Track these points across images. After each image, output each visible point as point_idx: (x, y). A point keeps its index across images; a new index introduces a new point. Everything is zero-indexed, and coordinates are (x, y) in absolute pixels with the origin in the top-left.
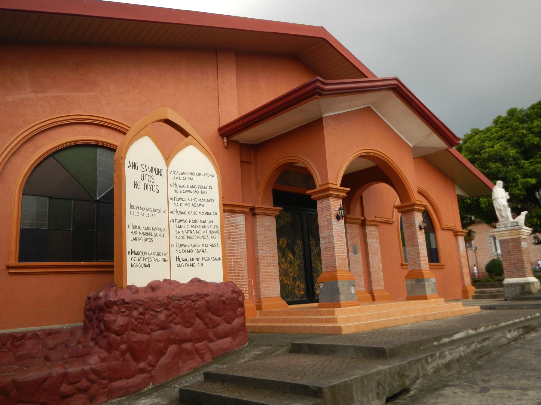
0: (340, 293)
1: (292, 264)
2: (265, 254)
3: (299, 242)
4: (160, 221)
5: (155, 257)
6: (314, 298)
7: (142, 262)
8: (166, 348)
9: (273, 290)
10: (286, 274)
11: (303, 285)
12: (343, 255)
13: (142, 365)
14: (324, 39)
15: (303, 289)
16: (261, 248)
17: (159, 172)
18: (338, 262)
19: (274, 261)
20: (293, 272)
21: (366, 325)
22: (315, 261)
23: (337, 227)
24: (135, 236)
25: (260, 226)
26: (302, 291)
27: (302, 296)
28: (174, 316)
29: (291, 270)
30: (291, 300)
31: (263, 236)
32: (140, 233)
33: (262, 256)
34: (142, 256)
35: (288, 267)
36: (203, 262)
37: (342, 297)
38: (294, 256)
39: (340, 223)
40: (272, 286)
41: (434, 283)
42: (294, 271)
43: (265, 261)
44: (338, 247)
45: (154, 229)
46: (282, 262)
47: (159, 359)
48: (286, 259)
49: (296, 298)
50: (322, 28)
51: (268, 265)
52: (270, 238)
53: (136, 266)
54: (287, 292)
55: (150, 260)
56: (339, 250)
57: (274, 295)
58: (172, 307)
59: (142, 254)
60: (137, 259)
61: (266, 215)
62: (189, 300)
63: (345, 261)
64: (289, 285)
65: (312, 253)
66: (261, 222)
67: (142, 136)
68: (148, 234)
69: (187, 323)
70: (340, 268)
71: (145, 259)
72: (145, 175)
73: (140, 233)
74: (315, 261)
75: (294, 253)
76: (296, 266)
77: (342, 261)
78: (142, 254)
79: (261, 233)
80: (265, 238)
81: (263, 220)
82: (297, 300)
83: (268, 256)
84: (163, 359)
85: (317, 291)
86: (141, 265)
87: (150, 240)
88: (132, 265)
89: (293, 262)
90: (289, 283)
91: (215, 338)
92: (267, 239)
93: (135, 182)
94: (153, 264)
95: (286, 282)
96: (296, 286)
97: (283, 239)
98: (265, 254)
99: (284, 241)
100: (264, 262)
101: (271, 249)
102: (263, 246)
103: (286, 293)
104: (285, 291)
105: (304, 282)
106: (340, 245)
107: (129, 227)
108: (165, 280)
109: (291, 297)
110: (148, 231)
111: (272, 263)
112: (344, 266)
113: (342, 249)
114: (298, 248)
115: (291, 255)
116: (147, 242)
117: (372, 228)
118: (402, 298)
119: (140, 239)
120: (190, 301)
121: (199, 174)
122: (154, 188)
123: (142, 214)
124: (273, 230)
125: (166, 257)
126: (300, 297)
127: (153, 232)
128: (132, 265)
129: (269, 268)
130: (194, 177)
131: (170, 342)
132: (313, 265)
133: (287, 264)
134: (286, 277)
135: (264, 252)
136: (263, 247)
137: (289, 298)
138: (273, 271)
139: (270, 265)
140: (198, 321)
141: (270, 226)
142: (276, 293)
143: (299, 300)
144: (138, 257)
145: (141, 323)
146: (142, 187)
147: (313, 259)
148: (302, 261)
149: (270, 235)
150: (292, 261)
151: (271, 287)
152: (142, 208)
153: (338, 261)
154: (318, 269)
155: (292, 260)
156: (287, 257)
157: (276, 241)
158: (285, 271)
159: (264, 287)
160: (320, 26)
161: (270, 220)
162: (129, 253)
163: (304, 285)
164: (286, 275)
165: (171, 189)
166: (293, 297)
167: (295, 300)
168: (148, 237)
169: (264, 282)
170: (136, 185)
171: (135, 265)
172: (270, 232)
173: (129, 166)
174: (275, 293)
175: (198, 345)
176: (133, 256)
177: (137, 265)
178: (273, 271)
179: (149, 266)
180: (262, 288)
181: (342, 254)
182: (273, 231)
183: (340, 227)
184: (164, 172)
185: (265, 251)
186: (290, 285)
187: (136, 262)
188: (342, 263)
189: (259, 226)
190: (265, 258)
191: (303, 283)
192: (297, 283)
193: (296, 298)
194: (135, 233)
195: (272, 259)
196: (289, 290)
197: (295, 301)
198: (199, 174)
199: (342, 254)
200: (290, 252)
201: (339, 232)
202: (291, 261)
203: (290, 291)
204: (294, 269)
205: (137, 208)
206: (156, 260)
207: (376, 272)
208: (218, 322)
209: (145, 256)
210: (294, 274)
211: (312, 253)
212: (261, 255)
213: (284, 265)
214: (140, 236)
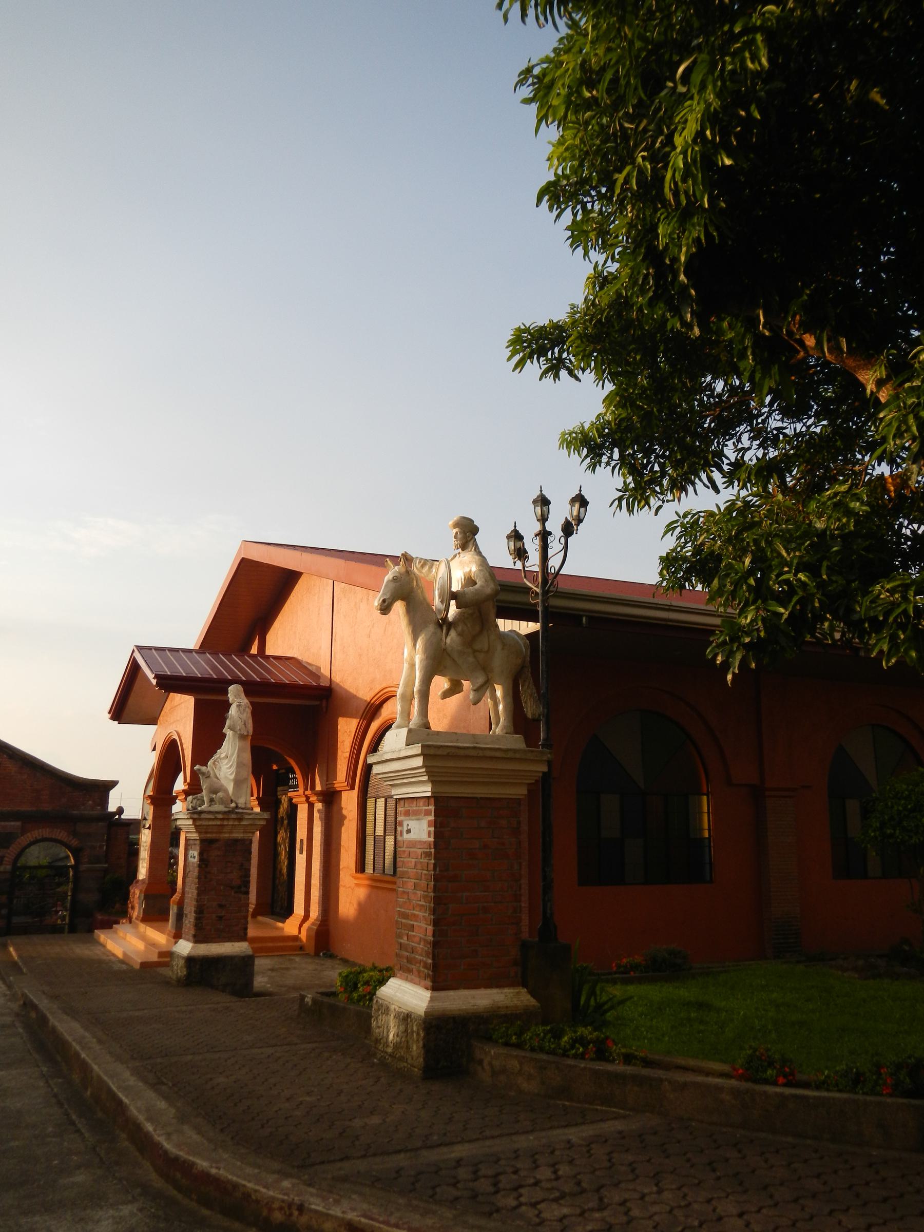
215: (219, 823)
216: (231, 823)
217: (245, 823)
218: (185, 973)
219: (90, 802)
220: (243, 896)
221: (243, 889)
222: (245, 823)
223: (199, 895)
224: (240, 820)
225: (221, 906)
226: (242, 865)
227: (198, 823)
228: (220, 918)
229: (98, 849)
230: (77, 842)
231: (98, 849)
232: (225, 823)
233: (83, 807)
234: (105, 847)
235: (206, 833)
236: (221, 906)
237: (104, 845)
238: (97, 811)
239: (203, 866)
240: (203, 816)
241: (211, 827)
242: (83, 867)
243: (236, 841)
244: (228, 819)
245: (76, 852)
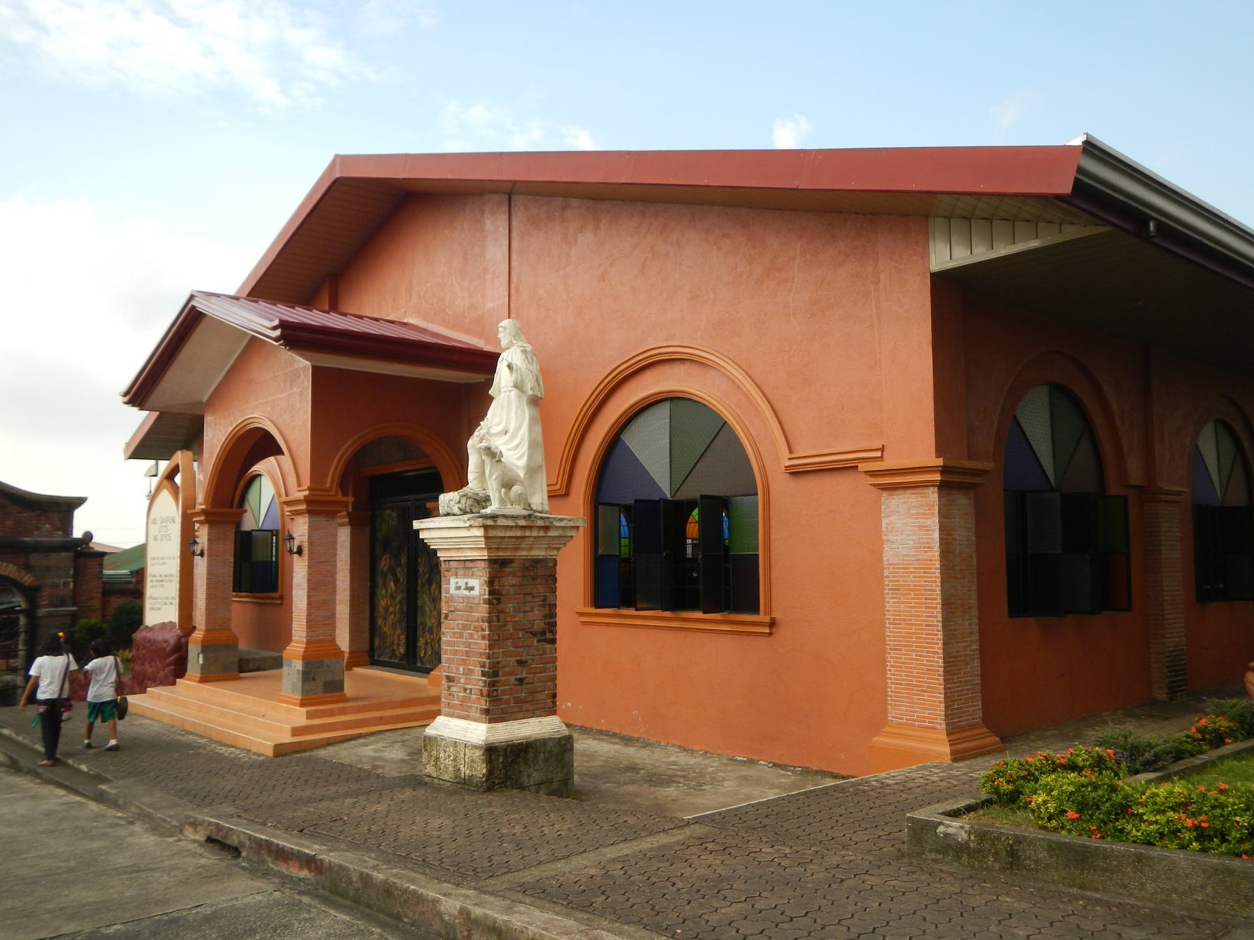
6: (415, 663)
38: (396, 585)
41: (298, 671)
45: (166, 576)
48: (386, 591)
50: (337, 157)
67: (161, 491)
82: (396, 661)
87: (162, 586)
94: (164, 607)
105: (405, 633)
114: (401, 573)
115: (392, 584)
118: (569, 704)
167: (393, 661)
168: (161, 583)
170: (156, 539)
176: (151, 601)
179: (160, 609)
192: (397, 633)
193: (395, 659)
194: (152, 581)
206: (166, 604)
210: (395, 616)
215: (519, 533)
216: (535, 534)
217: (552, 533)
218: (484, 771)
219: (47, 526)
220: (548, 646)
221: (549, 636)
222: (552, 533)
223: (491, 647)
224: (546, 528)
225: (521, 663)
226: (545, 599)
227: (492, 533)
228: (521, 681)
229: (62, 587)
230: (31, 580)
231: (62, 587)
232: (528, 534)
233: (36, 533)
234: (71, 585)
235: (498, 549)
236: (521, 663)
237: (69, 582)
238: (58, 537)
239: (495, 602)
240: (501, 522)
241: (507, 540)
242: (42, 612)
243: (536, 562)
244: (530, 528)
245: (31, 594)
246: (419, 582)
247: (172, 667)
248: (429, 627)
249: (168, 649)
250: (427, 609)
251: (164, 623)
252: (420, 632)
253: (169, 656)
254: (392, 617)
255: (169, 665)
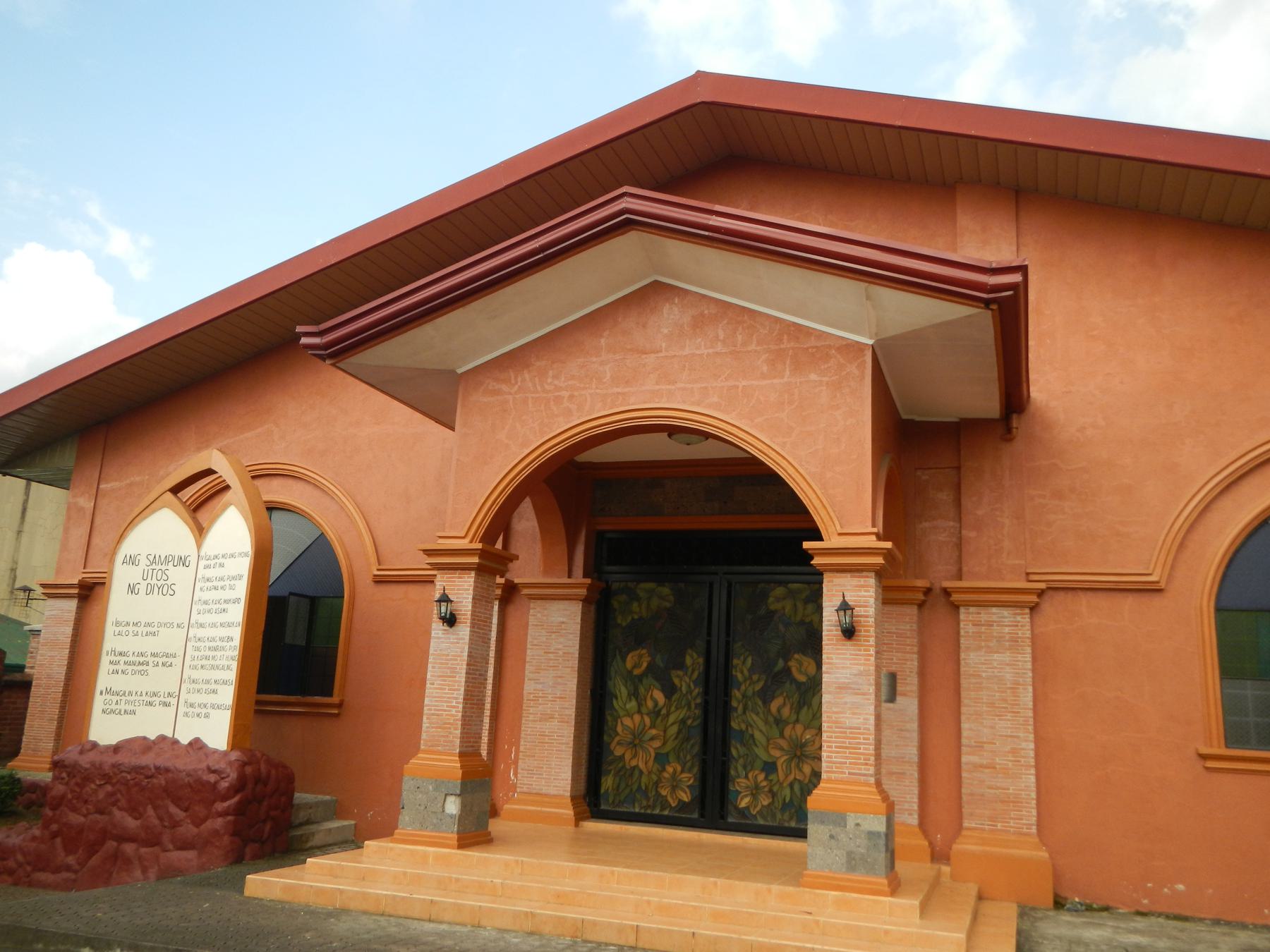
0: (403, 808)
1: (660, 719)
2: (542, 690)
3: (694, 660)
4: (170, 641)
5: (149, 699)
6: (723, 817)
7: (123, 707)
8: (102, 843)
9: (550, 779)
10: (637, 742)
11: (691, 775)
12: (447, 715)
13: (71, 860)
14: (703, 102)
15: (688, 787)
16: (532, 676)
17: (183, 561)
18: (426, 732)
19: (563, 708)
20: (662, 738)
21: (320, 892)
22: (744, 712)
23: (443, 642)
24: (115, 667)
25: (537, 625)
26: (686, 793)
27: (683, 806)
28: (119, 796)
29: (654, 732)
30: (643, 811)
31: (542, 649)
32: (125, 663)
33: (532, 695)
34: (123, 698)
35: (645, 726)
36: (210, 710)
37: (407, 818)
39: (453, 634)
40: (550, 768)
41: (871, 835)
42: (664, 737)
43: (538, 707)
44: (437, 693)
45: (153, 655)
46: (627, 710)
47: (90, 858)
48: (640, 705)
49: (663, 809)
51: (547, 717)
52: (561, 653)
53: (110, 713)
54: (635, 787)
55: (137, 704)
56: (436, 701)
57: (552, 791)
58: (118, 782)
59: (124, 694)
60: (114, 703)
61: (555, 599)
62: (141, 774)
63: (450, 728)
64: (641, 772)
65: (739, 690)
66: (539, 615)
68: (142, 664)
69: (134, 811)
70: (432, 746)
71: (129, 702)
72: (150, 572)
73: (125, 663)
74: (744, 712)
75: (669, 690)
76: (672, 724)
77: (440, 728)
78: (124, 694)
79: (535, 642)
80: (545, 653)
81: (546, 612)
82: (666, 813)
83: (550, 696)
84: (94, 858)
85: (742, 799)
86: (120, 711)
88: (104, 711)
89: (664, 712)
90: (641, 765)
91: (171, 847)
92: (551, 656)
93: (129, 585)
95: (634, 763)
96: (666, 775)
97: (638, 652)
98: (542, 690)
99: (640, 656)
100: (534, 709)
101: (559, 680)
102: (539, 673)
103: (631, 790)
104: (627, 785)
105: (695, 770)
106: (445, 689)
107: (107, 655)
108: (162, 738)
109: (644, 803)
110: (142, 659)
111: (557, 714)
112: (445, 741)
113: (448, 698)
115: (659, 696)
116: (138, 676)
117: (994, 614)
119: (123, 672)
120: (142, 777)
121: (232, 556)
122: (167, 589)
123: (135, 632)
124: (571, 634)
125: (168, 700)
126: (676, 807)
127: (150, 659)
128: (104, 711)
129: (548, 724)
130: (227, 562)
131: (104, 835)
132: (734, 725)
133: (642, 717)
134: (636, 753)
135: (540, 687)
136: (537, 674)
137: (636, 805)
138: (556, 732)
139: (550, 718)
140: (150, 811)
141: (563, 626)
142: (557, 787)
143: (671, 814)
144: (115, 698)
145: (77, 799)
146: (143, 592)
147: (736, 709)
148: (697, 711)
149: (560, 646)
150: (660, 710)
151: (545, 769)
152: (135, 624)
153: (428, 727)
154: (752, 736)
155: (662, 708)
156: (645, 700)
157: (575, 660)
158: (633, 734)
159: (527, 768)
160: (692, 72)
161: (564, 610)
162: (101, 693)
163: (694, 775)
164: (635, 746)
165: (198, 585)
166: (651, 803)
167: (657, 811)
168: (140, 668)
169: (529, 756)
170: (132, 589)
171: (109, 710)
172: (562, 640)
173: (123, 563)
174: (554, 786)
175: (143, 850)
176: (109, 697)
177: (113, 712)
178: (556, 732)
180: (522, 770)
181: (445, 711)
182: (571, 636)
183: (452, 643)
184: (193, 559)
185: (541, 683)
186: (644, 770)
187: (110, 707)
188: (441, 734)
189: (533, 625)
190: (540, 699)
191: (690, 771)
192: (670, 770)
193: (663, 809)
195: (558, 703)
196: (640, 783)
197: (656, 815)
198: (232, 556)
199: (445, 711)
200: (657, 685)
201: (448, 655)
202: (657, 709)
203: (644, 788)
204: (665, 731)
205: (128, 624)
206: (150, 704)
207: (995, 768)
208: (178, 819)
209: (129, 698)
210: (664, 744)
211: (739, 690)
212: (531, 693)
213: (632, 718)
214: (125, 667)
246: (737, 694)
247: (230, 818)
248: (766, 763)
249: (224, 784)
250: (757, 735)
251: (145, 738)
252: (737, 769)
253: (224, 799)
254: (657, 744)
255: (220, 815)
